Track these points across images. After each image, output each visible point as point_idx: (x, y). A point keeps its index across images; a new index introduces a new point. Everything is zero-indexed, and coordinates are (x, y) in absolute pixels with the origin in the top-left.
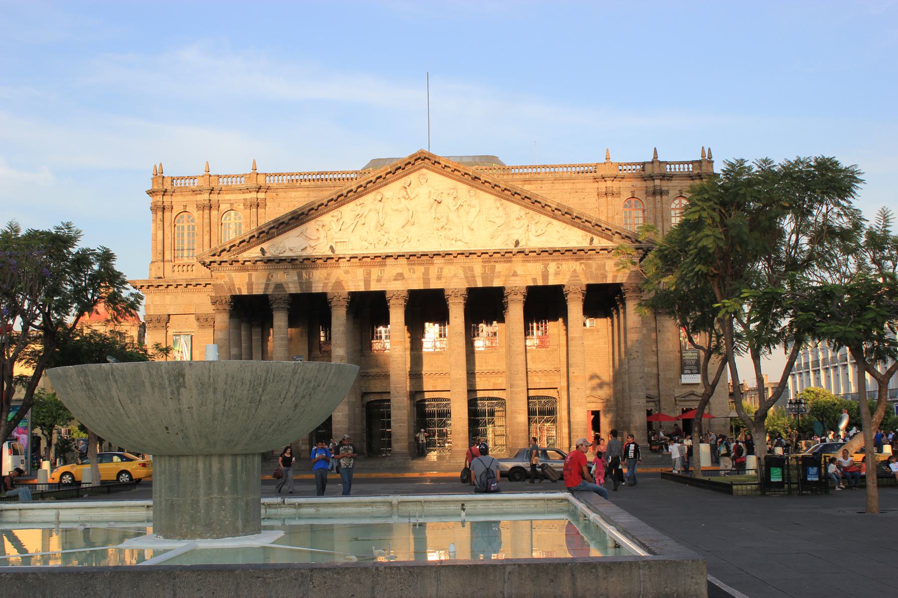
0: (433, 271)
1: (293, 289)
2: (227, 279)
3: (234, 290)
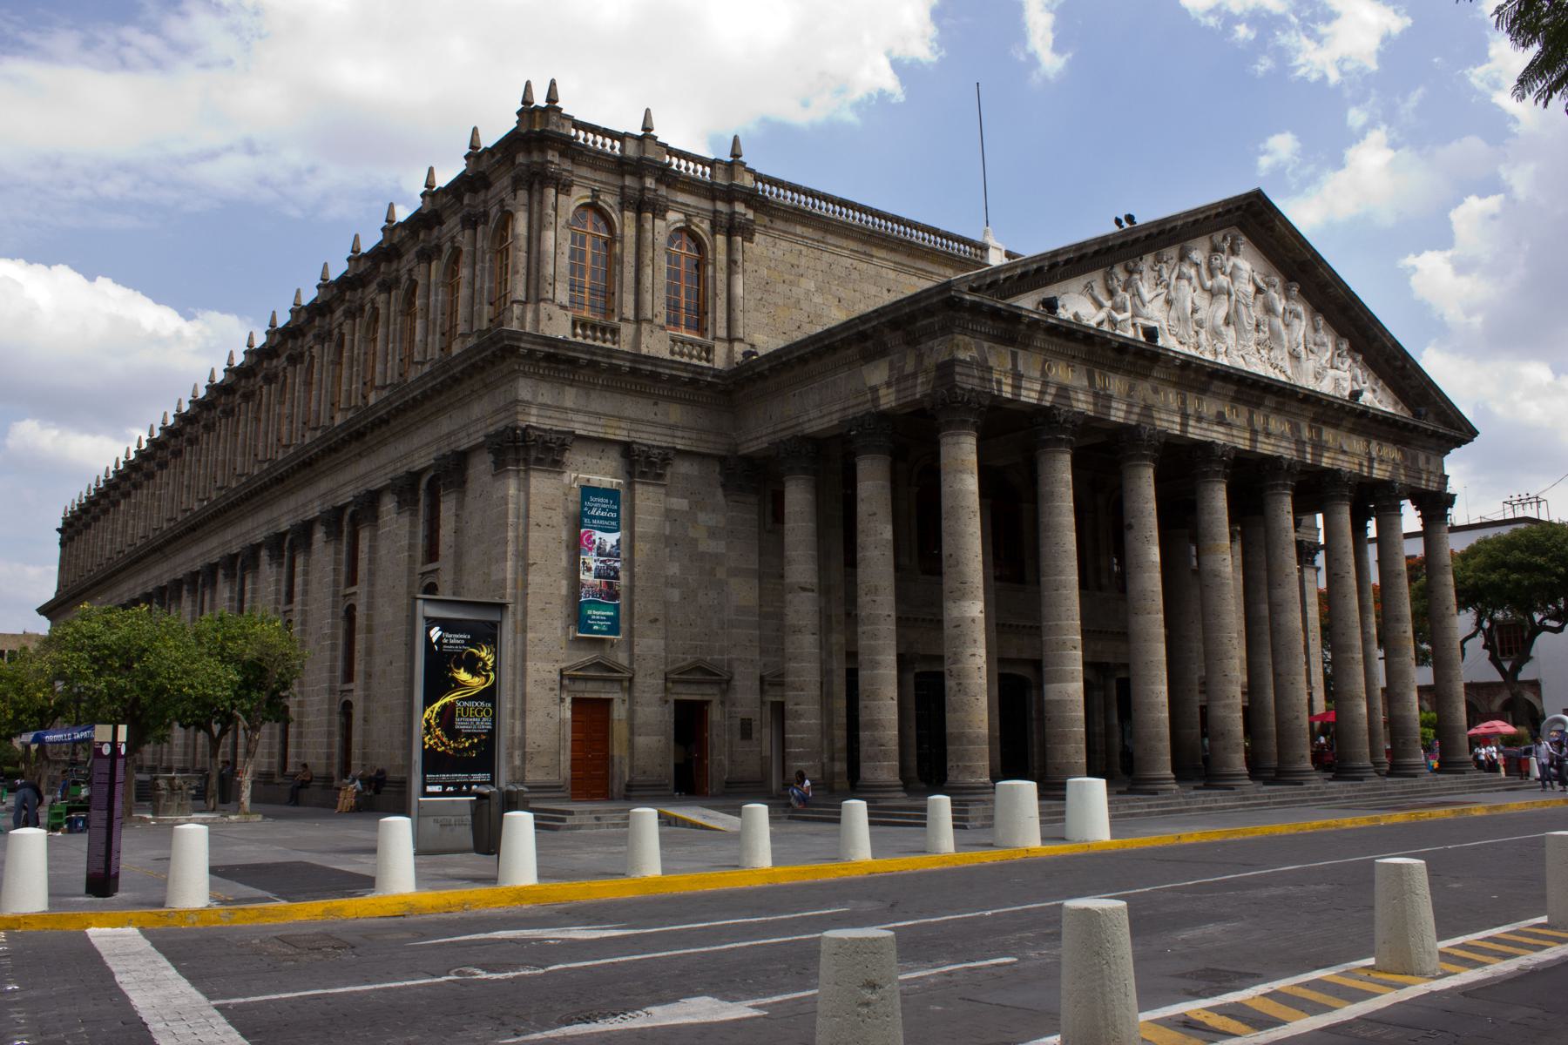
0: (1259, 420)
1: (1083, 403)
2: (975, 353)
3: (990, 381)
